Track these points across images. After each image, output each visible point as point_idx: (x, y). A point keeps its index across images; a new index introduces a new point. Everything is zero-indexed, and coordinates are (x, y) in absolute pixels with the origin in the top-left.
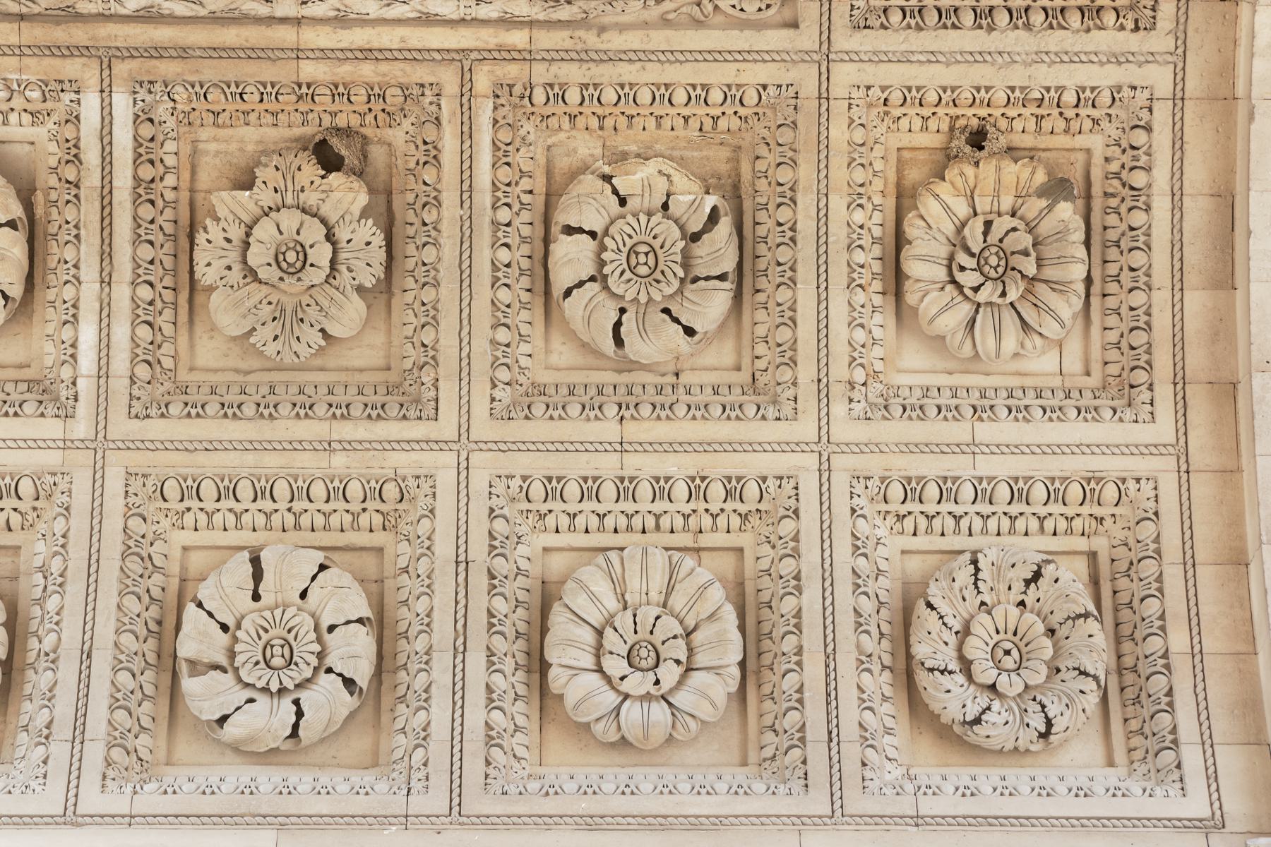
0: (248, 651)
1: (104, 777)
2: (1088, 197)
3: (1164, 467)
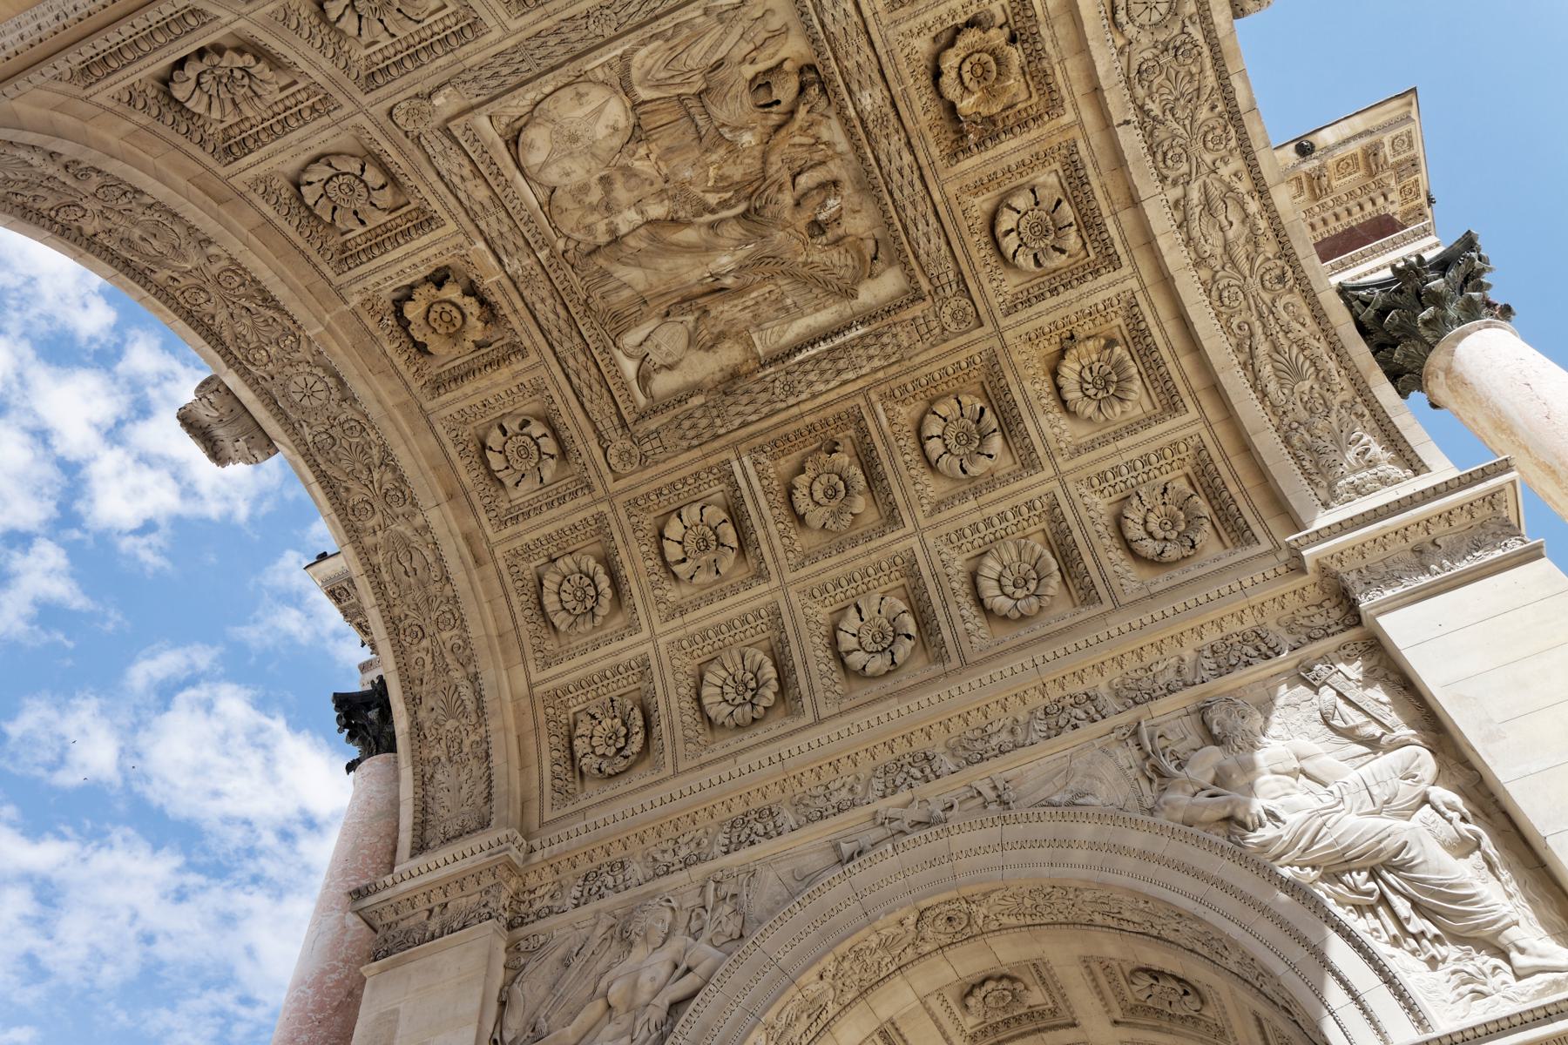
0: (867, 640)
2: (1127, 343)
3: (1199, 427)
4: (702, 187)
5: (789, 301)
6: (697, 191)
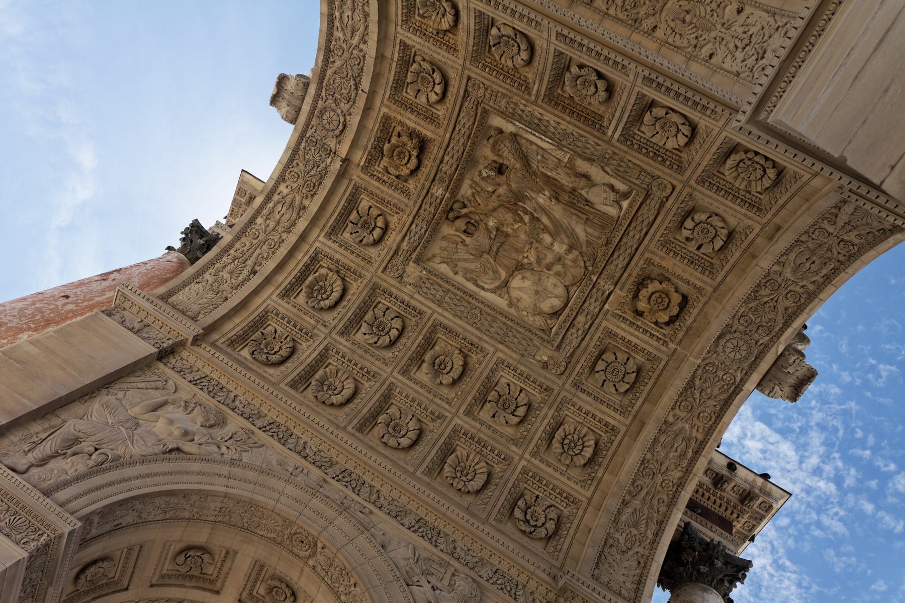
4: (524, 226)
5: (539, 158)
6: (527, 228)
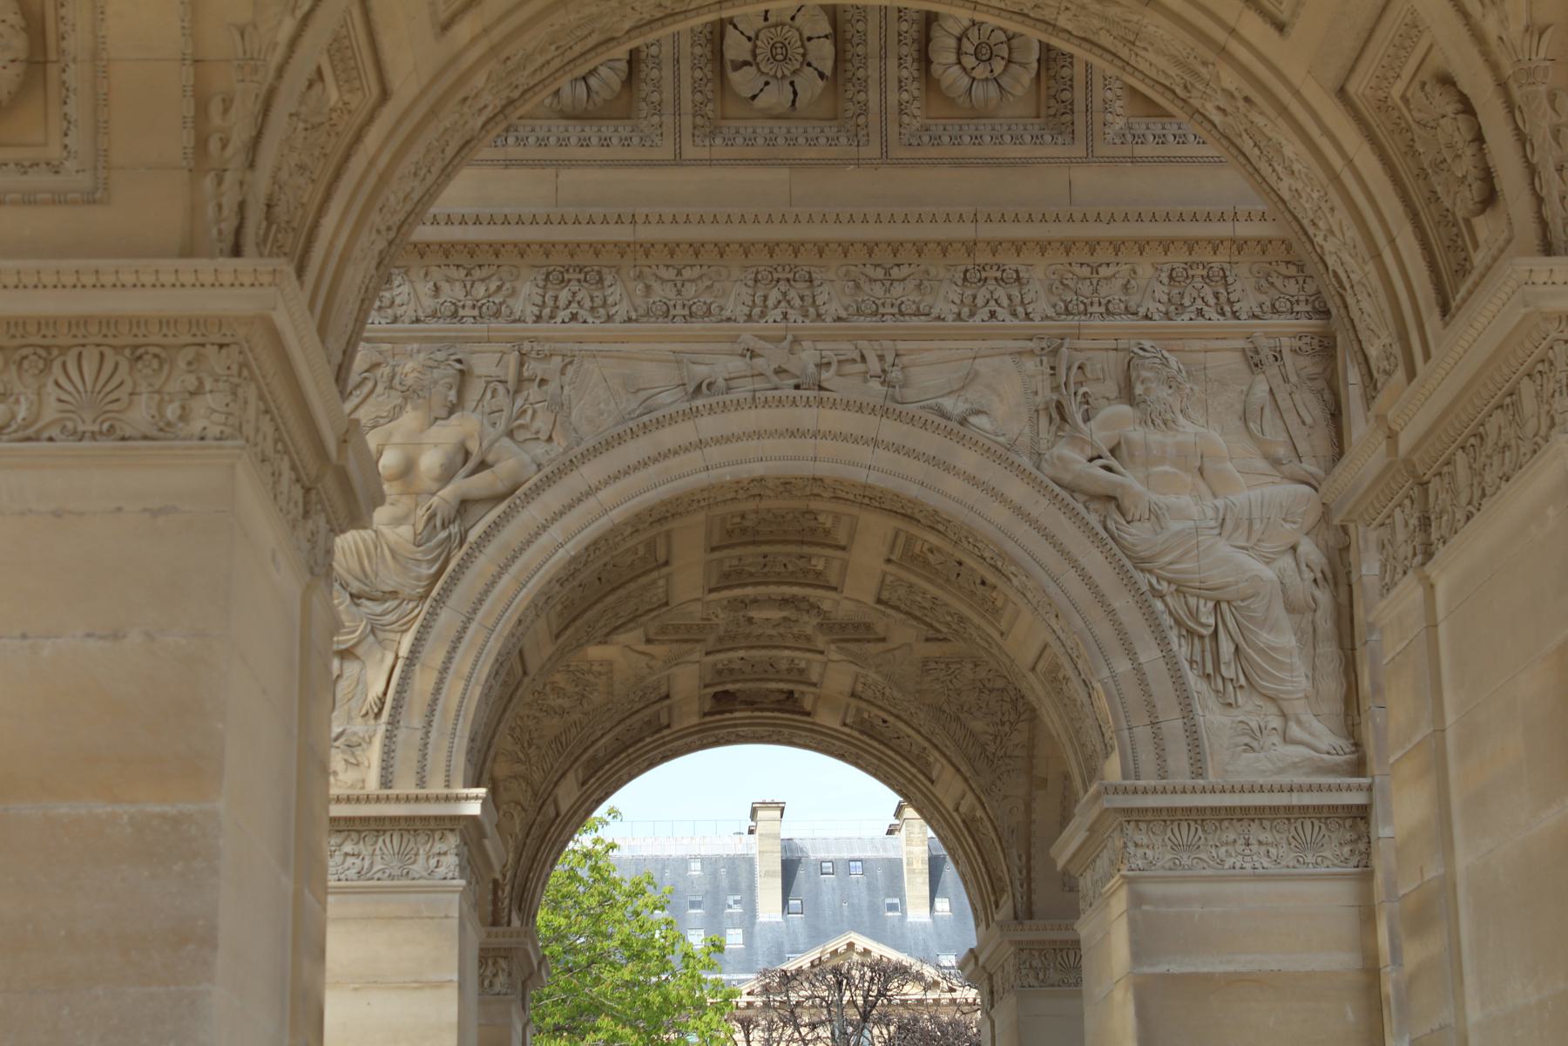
0: (763, 51)
1: (693, 135)
